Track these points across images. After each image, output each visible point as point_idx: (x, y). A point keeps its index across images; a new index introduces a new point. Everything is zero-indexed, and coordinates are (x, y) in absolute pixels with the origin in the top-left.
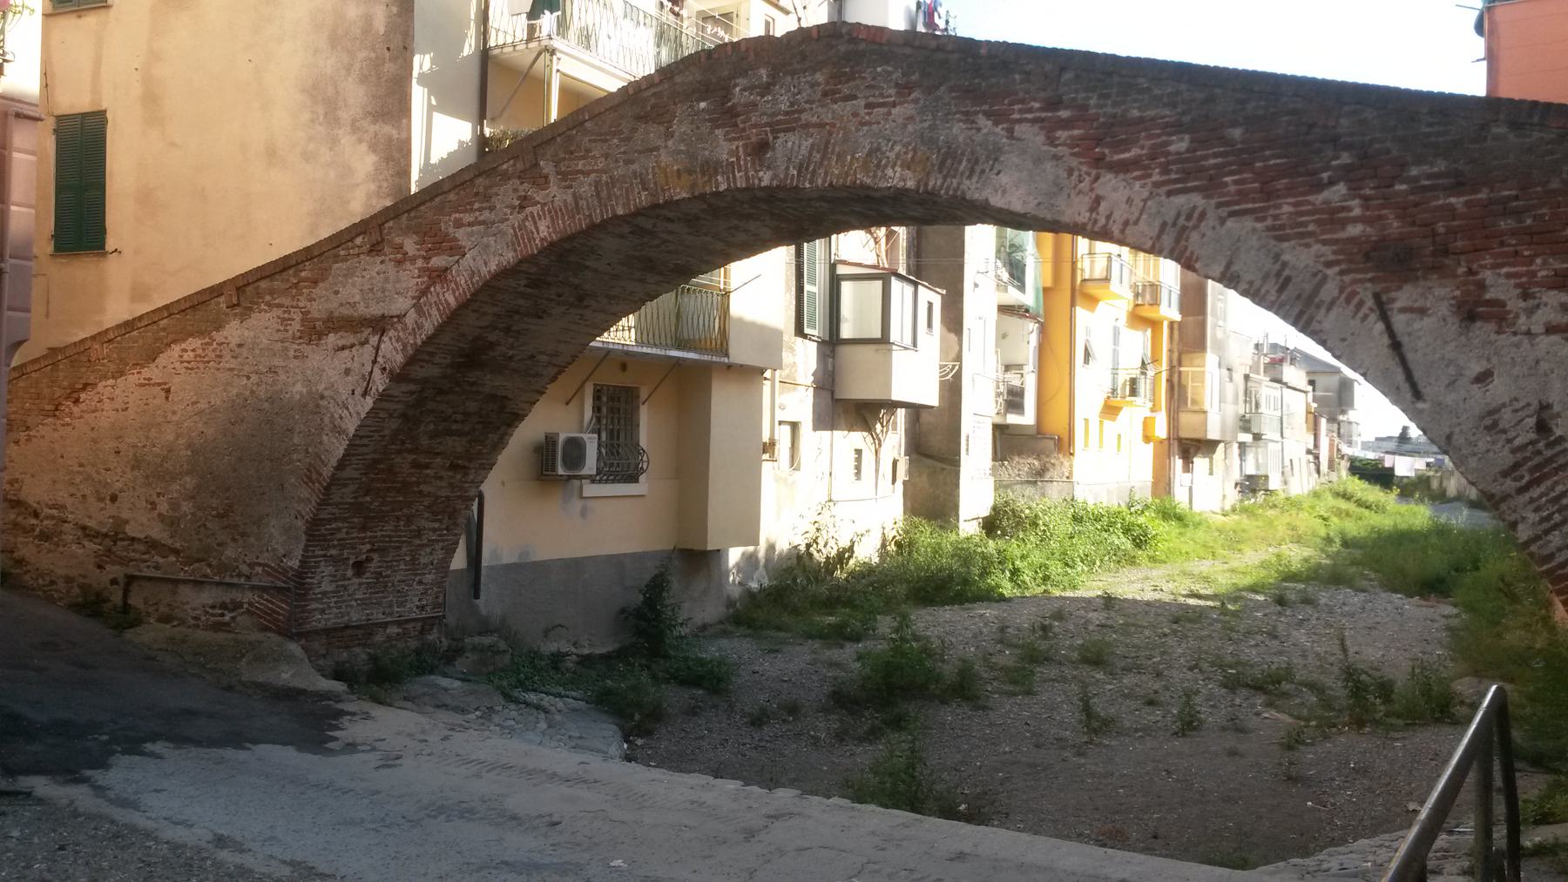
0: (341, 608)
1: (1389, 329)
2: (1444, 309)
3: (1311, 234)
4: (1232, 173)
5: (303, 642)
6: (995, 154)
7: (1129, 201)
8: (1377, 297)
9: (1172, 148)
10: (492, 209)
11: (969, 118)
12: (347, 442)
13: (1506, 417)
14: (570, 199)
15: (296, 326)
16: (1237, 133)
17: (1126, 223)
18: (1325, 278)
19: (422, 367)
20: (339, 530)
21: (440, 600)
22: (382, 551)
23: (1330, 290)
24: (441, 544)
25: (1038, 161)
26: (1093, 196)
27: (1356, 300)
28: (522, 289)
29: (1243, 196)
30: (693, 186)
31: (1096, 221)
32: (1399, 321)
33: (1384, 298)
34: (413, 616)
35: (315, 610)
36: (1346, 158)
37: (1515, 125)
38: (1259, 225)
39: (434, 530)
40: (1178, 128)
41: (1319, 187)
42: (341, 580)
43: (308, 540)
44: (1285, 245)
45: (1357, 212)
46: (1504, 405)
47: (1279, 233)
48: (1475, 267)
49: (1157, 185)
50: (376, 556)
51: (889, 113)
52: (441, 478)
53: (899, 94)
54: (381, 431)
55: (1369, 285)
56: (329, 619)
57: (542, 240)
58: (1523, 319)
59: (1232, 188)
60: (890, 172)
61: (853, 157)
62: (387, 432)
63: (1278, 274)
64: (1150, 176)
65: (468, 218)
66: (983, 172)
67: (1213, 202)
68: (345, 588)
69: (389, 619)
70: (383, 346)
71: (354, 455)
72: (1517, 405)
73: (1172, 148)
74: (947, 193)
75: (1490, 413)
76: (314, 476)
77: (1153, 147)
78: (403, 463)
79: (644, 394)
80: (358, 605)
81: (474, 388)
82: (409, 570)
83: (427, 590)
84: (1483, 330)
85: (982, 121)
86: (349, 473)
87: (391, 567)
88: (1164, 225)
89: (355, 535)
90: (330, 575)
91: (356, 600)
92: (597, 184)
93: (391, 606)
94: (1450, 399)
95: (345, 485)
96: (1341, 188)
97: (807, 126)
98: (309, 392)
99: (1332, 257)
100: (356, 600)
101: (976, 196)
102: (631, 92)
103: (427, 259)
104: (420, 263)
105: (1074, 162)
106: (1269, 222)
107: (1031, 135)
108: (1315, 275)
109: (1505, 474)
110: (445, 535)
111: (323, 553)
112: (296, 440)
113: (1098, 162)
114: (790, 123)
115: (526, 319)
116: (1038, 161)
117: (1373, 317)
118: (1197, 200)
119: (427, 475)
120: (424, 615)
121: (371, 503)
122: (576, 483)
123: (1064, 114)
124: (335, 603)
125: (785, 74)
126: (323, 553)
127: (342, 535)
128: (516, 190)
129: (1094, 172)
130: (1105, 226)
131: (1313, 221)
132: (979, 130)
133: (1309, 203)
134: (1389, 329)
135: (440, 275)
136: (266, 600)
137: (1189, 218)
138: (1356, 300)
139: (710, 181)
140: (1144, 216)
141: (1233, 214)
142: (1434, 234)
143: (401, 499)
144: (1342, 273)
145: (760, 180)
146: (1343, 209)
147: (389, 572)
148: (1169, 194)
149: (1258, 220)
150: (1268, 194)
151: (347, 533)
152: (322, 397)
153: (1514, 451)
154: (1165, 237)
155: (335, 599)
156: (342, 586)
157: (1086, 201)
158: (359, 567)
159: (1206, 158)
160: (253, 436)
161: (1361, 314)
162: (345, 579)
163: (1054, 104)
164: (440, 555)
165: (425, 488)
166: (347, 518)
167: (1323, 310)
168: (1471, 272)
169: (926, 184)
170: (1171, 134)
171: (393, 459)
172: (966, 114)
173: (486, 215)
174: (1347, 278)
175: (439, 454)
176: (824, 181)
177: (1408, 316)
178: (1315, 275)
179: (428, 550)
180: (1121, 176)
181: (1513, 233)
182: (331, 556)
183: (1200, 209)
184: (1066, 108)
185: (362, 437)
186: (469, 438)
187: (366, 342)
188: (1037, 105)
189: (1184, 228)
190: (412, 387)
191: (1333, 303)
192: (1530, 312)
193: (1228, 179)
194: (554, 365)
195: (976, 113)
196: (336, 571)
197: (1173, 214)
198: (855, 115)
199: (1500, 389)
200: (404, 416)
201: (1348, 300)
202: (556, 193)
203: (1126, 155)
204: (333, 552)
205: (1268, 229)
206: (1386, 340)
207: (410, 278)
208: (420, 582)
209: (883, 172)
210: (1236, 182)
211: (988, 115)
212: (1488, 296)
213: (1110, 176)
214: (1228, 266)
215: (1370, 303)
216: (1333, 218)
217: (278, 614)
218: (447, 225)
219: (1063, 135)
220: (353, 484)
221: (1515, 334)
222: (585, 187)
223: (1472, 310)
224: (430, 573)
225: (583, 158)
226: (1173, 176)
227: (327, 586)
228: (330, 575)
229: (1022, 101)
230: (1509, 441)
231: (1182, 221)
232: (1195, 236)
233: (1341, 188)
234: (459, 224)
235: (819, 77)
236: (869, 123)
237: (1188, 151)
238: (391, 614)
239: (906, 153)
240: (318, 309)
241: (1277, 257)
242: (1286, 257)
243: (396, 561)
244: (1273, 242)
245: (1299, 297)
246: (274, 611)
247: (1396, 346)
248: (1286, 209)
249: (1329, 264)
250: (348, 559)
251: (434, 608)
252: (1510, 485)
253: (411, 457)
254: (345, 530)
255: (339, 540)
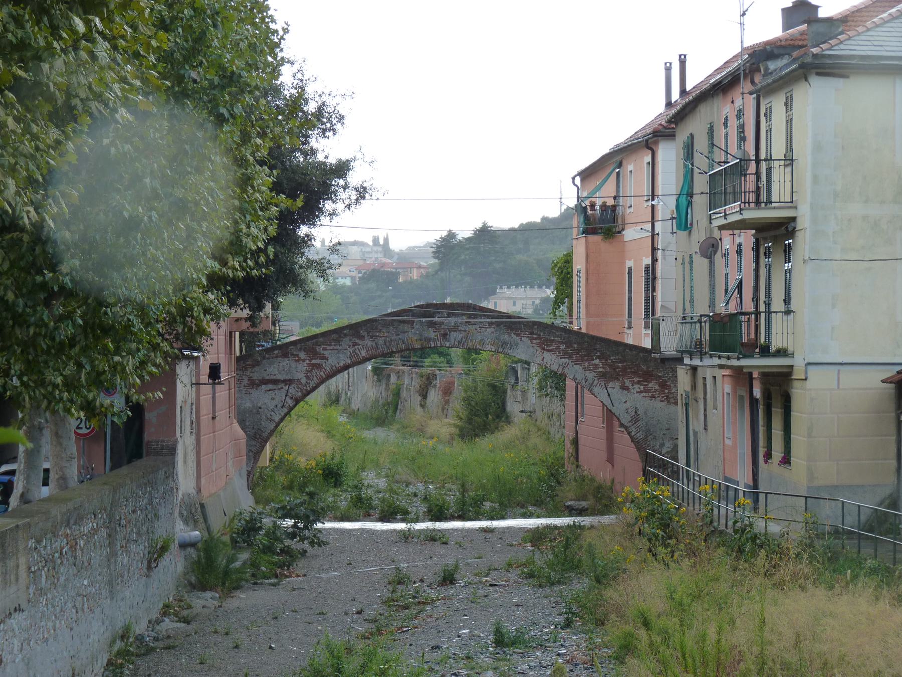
2: (618, 387)
6: (517, 345)
10: (340, 345)
11: (509, 334)
13: (630, 410)
14: (374, 345)
15: (246, 382)
16: (575, 346)
23: (596, 382)
25: (528, 347)
30: (422, 345)
32: (609, 389)
36: (598, 354)
37: (631, 350)
40: (562, 343)
41: (593, 360)
47: (585, 369)
57: (363, 357)
65: (329, 348)
70: (290, 390)
76: (258, 437)
85: (513, 335)
92: (385, 341)
96: (598, 360)
97: (461, 331)
98: (253, 406)
103: (310, 360)
104: (308, 361)
105: (538, 348)
112: (247, 424)
113: (543, 349)
114: (455, 329)
116: (528, 347)
118: (567, 360)
123: (535, 336)
128: (350, 340)
135: (318, 366)
150: (583, 360)
152: (260, 408)
157: (541, 358)
163: (532, 333)
173: (338, 347)
181: (631, 372)
187: (282, 388)
199: (628, 405)
202: (369, 343)
207: (303, 367)
211: (515, 334)
216: (596, 367)
218: (319, 349)
219: (534, 341)
222: (381, 342)
223: (624, 388)
225: (379, 332)
233: (598, 360)
234: (325, 349)
240: (256, 376)
247: (609, 395)
252: (630, 424)
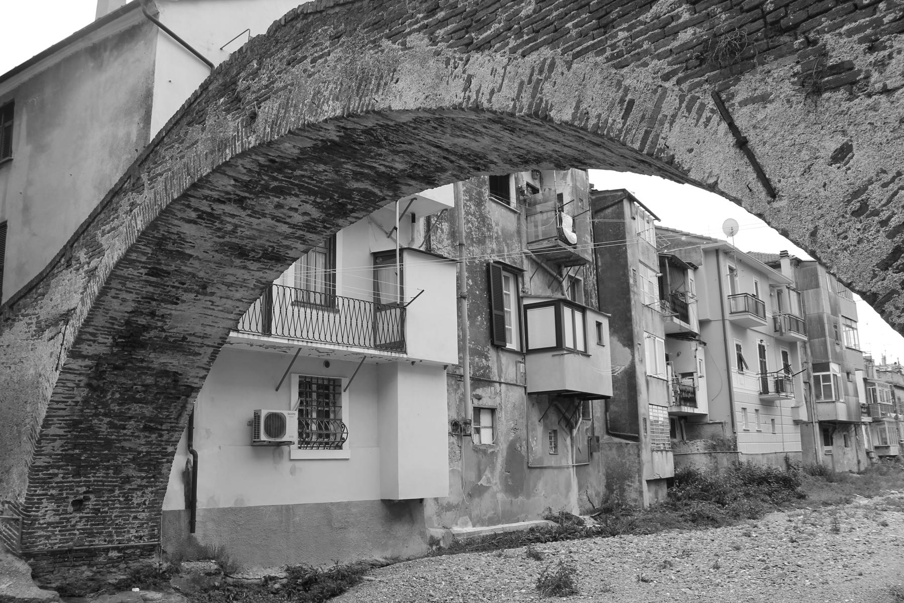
0: (65, 535)
1: (733, 128)
2: (787, 88)
3: (646, 52)
4: (571, 19)
5: (32, 560)
7: (493, 72)
8: (716, 96)
9: (523, 14)
11: (376, 44)
12: (47, 406)
17: (492, 92)
18: (665, 90)
19: (90, 345)
20: (56, 475)
21: (156, 532)
22: (98, 492)
23: (670, 103)
24: (150, 489)
26: (466, 76)
27: (697, 105)
28: (144, 277)
29: (583, 35)
31: (469, 98)
32: (742, 118)
33: (724, 97)
34: (132, 543)
35: (40, 536)
38: (599, 59)
39: (142, 478)
42: (62, 514)
43: (30, 482)
44: (626, 70)
45: (686, 16)
46: (870, 182)
48: (812, 35)
49: (513, 51)
50: (92, 496)
51: (326, 61)
52: (138, 437)
53: (332, 44)
54: (73, 398)
55: (706, 86)
56: (55, 544)
58: (875, 76)
59: (573, 33)
60: (325, 108)
61: (303, 103)
62: (79, 399)
63: (622, 101)
64: (508, 44)
66: (386, 84)
67: (559, 50)
68: (68, 520)
69: (110, 545)
71: (54, 416)
72: (886, 178)
73: (523, 14)
74: (362, 111)
75: (856, 194)
77: (508, 20)
78: (103, 426)
79: (344, 382)
80: (81, 534)
81: (144, 364)
82: (124, 508)
83: (143, 524)
84: (834, 99)
85: (386, 43)
86: (53, 430)
87: (108, 505)
88: (522, 84)
89: (71, 479)
90: (53, 510)
91: (78, 530)
93: (111, 536)
94: (808, 187)
95: (55, 440)
99: (668, 69)
100: (78, 530)
101: (382, 106)
102: (186, 107)
105: (450, 53)
106: (608, 53)
107: (419, 41)
108: (655, 91)
109: (885, 265)
110: (153, 482)
111: (44, 492)
113: (469, 46)
115: (162, 304)
116: (423, 62)
117: (716, 118)
118: (546, 52)
119: (125, 435)
120: (142, 543)
121: (80, 455)
122: (285, 448)
123: (441, 15)
124: (60, 531)
125: (266, 58)
126: (44, 492)
127: (58, 479)
129: (465, 56)
130: (476, 100)
131: (646, 39)
132: (382, 51)
133: (641, 23)
134: (733, 128)
136: (8, 529)
137: (541, 72)
138: (697, 105)
139: (222, 155)
140: (506, 81)
141: (577, 56)
142: (764, 15)
143: (106, 452)
144: (679, 82)
145: (250, 143)
146: (672, 18)
147: (106, 509)
148: (524, 56)
149: (598, 54)
150: (605, 26)
151: (63, 478)
153: (891, 235)
154: (523, 95)
155: (59, 528)
156: (64, 518)
158: (79, 505)
159: (551, 11)
160: (10, 409)
161: (703, 120)
162: (67, 513)
164: (149, 497)
165: (127, 445)
166: (62, 466)
167: (667, 125)
168: (809, 42)
169: (349, 108)
170: (518, 4)
171: (91, 420)
172: (374, 42)
174: (685, 86)
175: (130, 418)
176: (285, 130)
177: (750, 107)
178: (655, 91)
179: (139, 493)
180: (487, 52)
182: (52, 495)
183: (548, 62)
184: (442, 10)
185: (58, 402)
186: (154, 405)
188: (421, 16)
189: (539, 81)
190: (88, 362)
191: (674, 116)
192: (881, 65)
193: (569, 25)
194: (208, 346)
195: (381, 38)
196: (58, 506)
197: (528, 72)
198: (305, 71)
200: (89, 385)
201: (689, 110)
203: (489, 32)
204: (53, 492)
205: (608, 60)
206: (731, 139)
208: (135, 518)
209: (321, 109)
210: (576, 26)
211: (389, 37)
212: (831, 62)
213: (477, 55)
214: (577, 107)
215: (711, 104)
217: (14, 539)
219: (440, 32)
220: (60, 439)
221: (869, 96)
224: (143, 511)
226: (526, 37)
227: (50, 518)
228: (53, 510)
229: (412, 16)
230: (884, 223)
231: (535, 77)
232: (547, 86)
235: (285, 52)
236: (314, 73)
237: (535, 12)
238: (111, 542)
239: (336, 88)
241: (619, 83)
242: (627, 82)
243: (111, 501)
244: (614, 71)
245: (643, 117)
246: (11, 536)
247: (742, 144)
248: (622, 35)
249: (666, 77)
250: (67, 498)
251: (151, 539)
253: (106, 420)
254: (62, 475)
255: (57, 483)
